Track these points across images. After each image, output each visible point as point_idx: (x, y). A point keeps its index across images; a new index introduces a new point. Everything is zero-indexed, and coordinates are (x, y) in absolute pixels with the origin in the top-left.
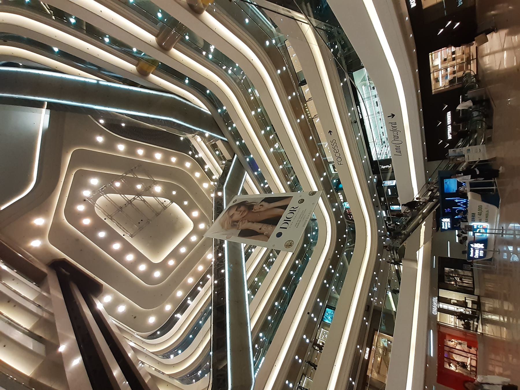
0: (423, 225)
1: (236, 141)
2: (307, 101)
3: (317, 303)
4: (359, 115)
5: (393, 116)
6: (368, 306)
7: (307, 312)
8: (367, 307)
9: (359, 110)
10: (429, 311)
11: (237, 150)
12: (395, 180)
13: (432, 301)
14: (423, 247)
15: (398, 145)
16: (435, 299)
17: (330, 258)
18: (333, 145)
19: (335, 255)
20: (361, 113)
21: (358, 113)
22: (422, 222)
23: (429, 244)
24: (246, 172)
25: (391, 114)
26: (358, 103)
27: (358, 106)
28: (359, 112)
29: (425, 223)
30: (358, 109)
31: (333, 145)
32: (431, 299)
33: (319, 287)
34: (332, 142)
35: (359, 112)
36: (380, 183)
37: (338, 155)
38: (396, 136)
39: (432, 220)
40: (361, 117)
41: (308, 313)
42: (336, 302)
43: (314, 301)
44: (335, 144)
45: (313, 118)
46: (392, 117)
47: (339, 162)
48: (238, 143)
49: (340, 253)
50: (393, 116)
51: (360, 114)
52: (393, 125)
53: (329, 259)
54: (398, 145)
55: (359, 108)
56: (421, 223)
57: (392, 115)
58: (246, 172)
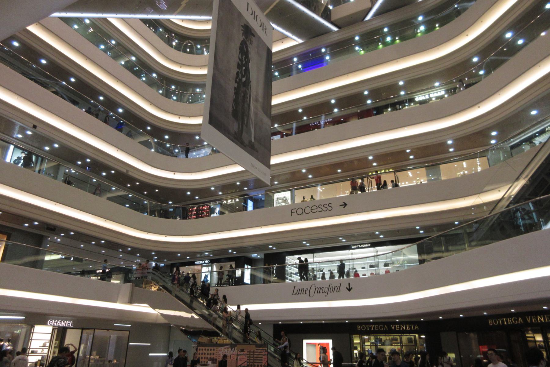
0: (193, 315)
1: (361, 36)
2: (395, 174)
3: (50, 142)
4: (356, 245)
5: (349, 289)
6: (55, 228)
7: (36, 123)
8: (52, 228)
9: (364, 246)
10: (51, 315)
11: (345, 34)
12: (251, 283)
13: (67, 320)
14: (157, 313)
15: (308, 292)
16: (68, 324)
17: (130, 173)
18: (325, 206)
19: (132, 180)
20: (359, 248)
21: (360, 244)
22: (197, 314)
23: (163, 321)
24: (300, 41)
25: (352, 288)
26: (374, 245)
27: (369, 245)
28: (361, 246)
29: (196, 317)
30: (365, 244)
31: (325, 206)
32: (69, 318)
33: (78, 148)
34: (330, 205)
35: (361, 246)
36: (251, 262)
37: (308, 210)
38: (321, 290)
39: (201, 327)
40: (353, 247)
41: (35, 127)
42: (49, 175)
43: (56, 137)
44: (325, 209)
45: (368, 178)
46: (348, 288)
47: (295, 211)
48: (357, 38)
49: (134, 189)
50: (349, 289)
51: (357, 246)
52: (336, 288)
53: (127, 171)
54: (308, 292)
55: (367, 245)
56: (194, 312)
57: (351, 287)
58: (300, 41)
